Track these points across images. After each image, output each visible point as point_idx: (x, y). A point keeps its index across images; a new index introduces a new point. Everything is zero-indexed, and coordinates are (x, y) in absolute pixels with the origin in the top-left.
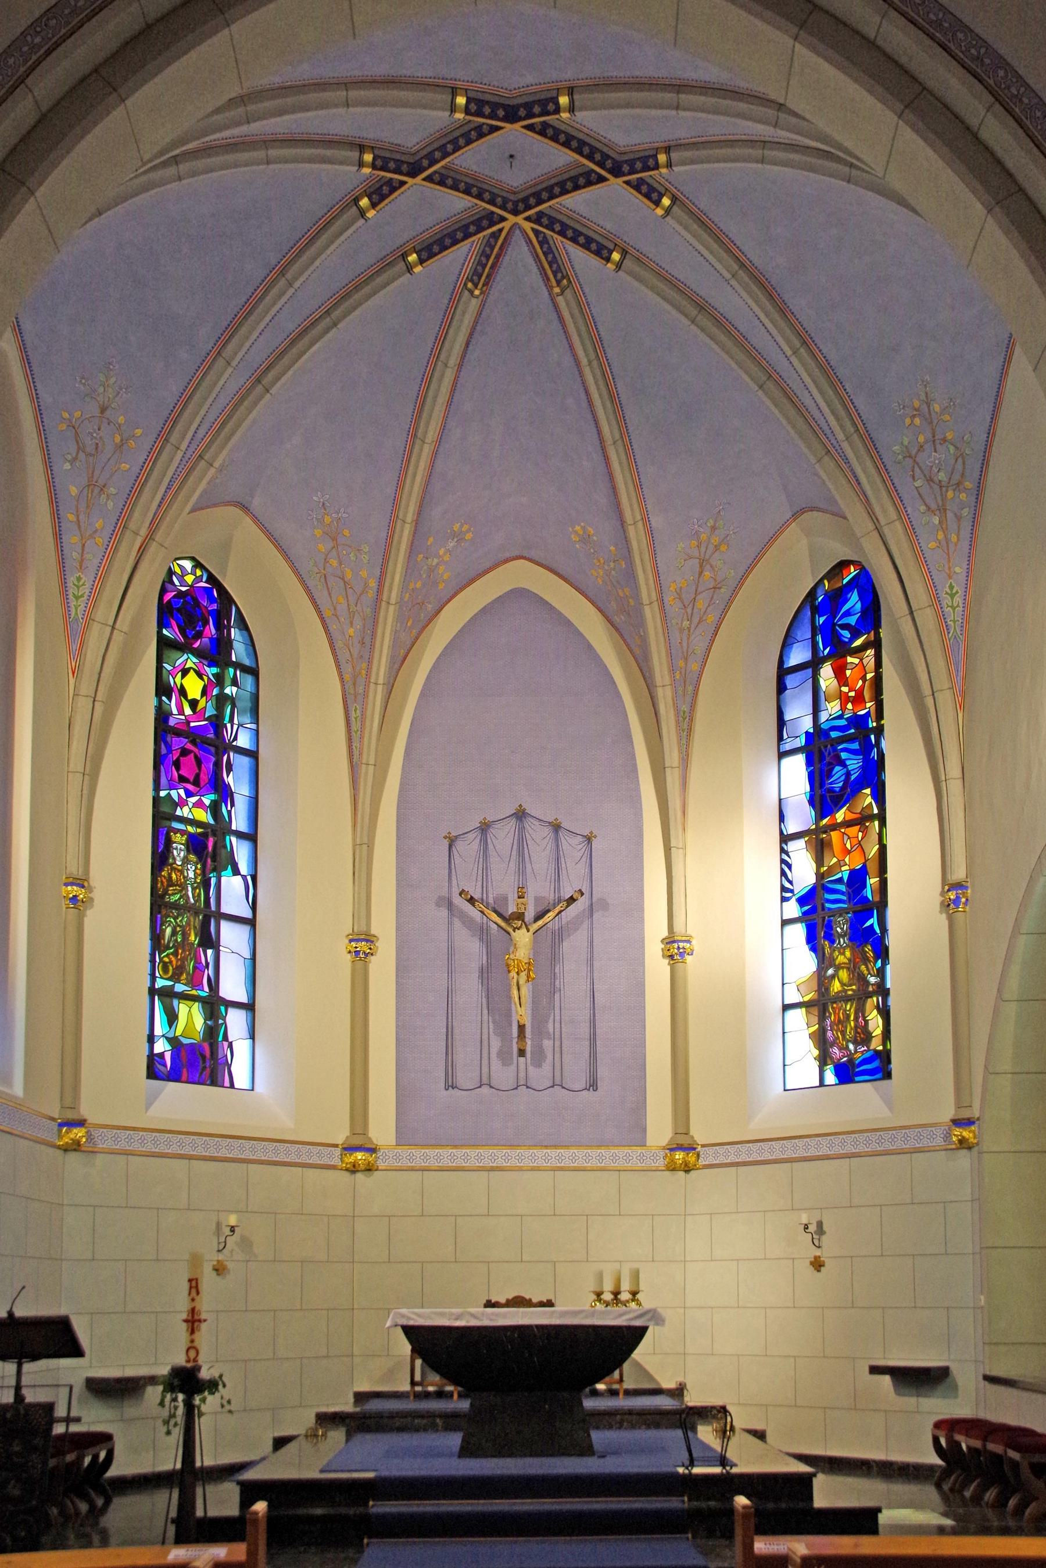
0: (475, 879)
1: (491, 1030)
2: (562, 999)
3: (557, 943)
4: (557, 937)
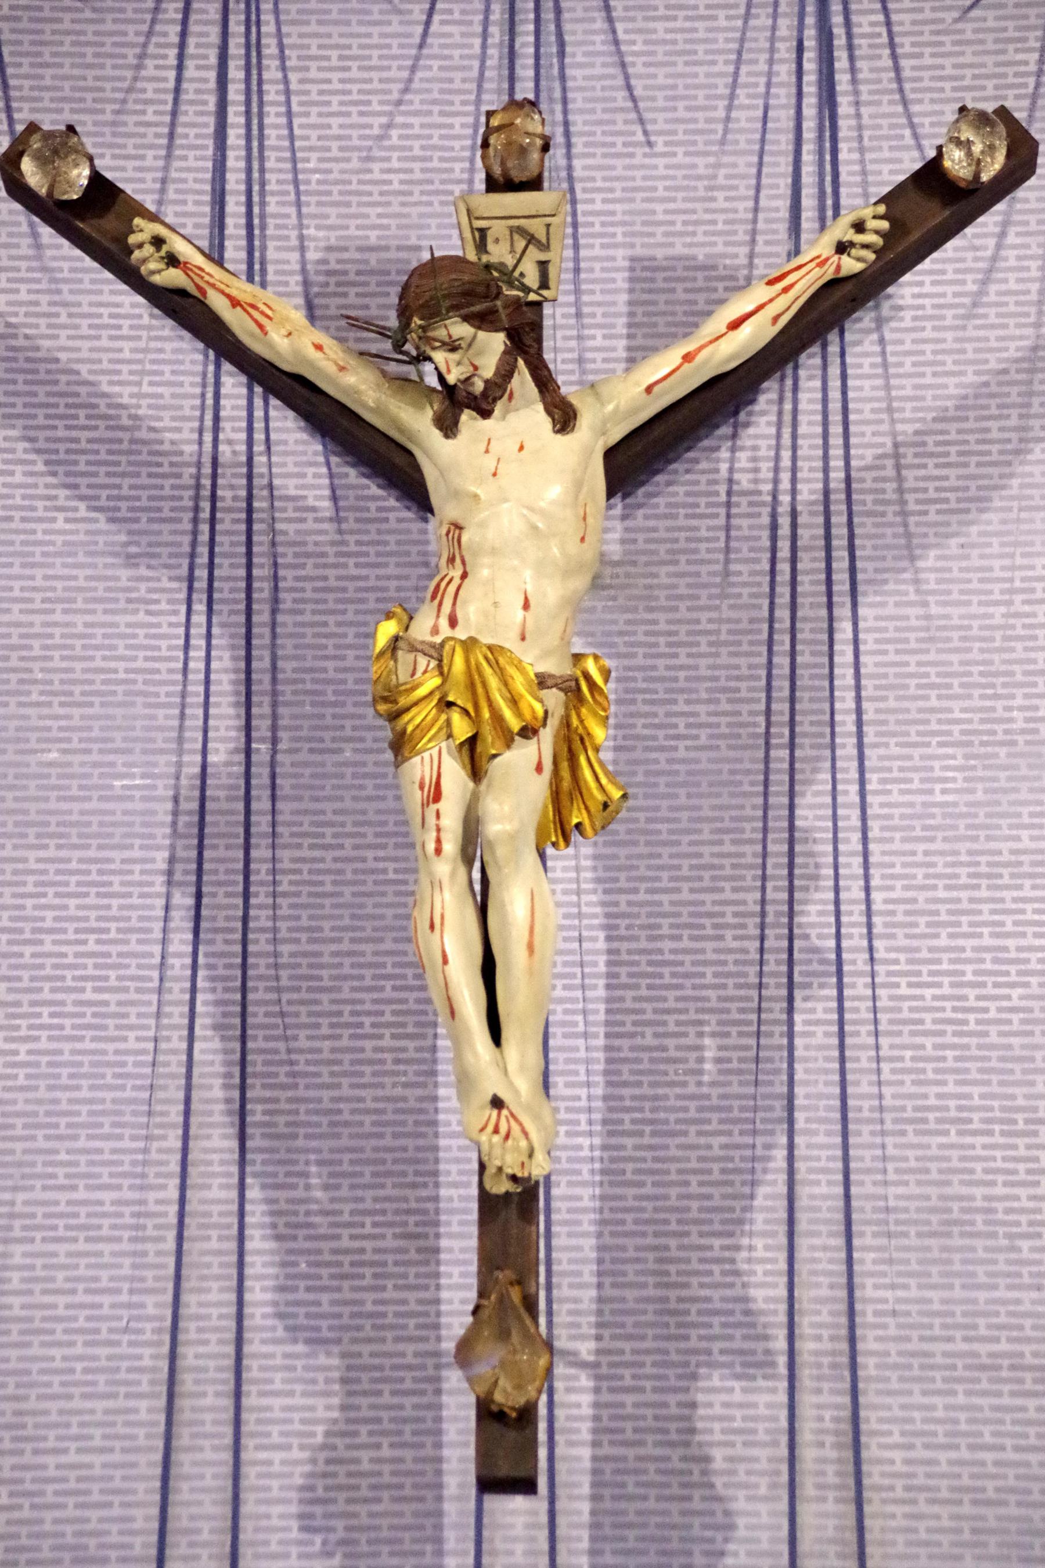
0: (156, 134)
1: (257, 1294)
2: (860, 1036)
3: (812, 608)
4: (810, 562)
